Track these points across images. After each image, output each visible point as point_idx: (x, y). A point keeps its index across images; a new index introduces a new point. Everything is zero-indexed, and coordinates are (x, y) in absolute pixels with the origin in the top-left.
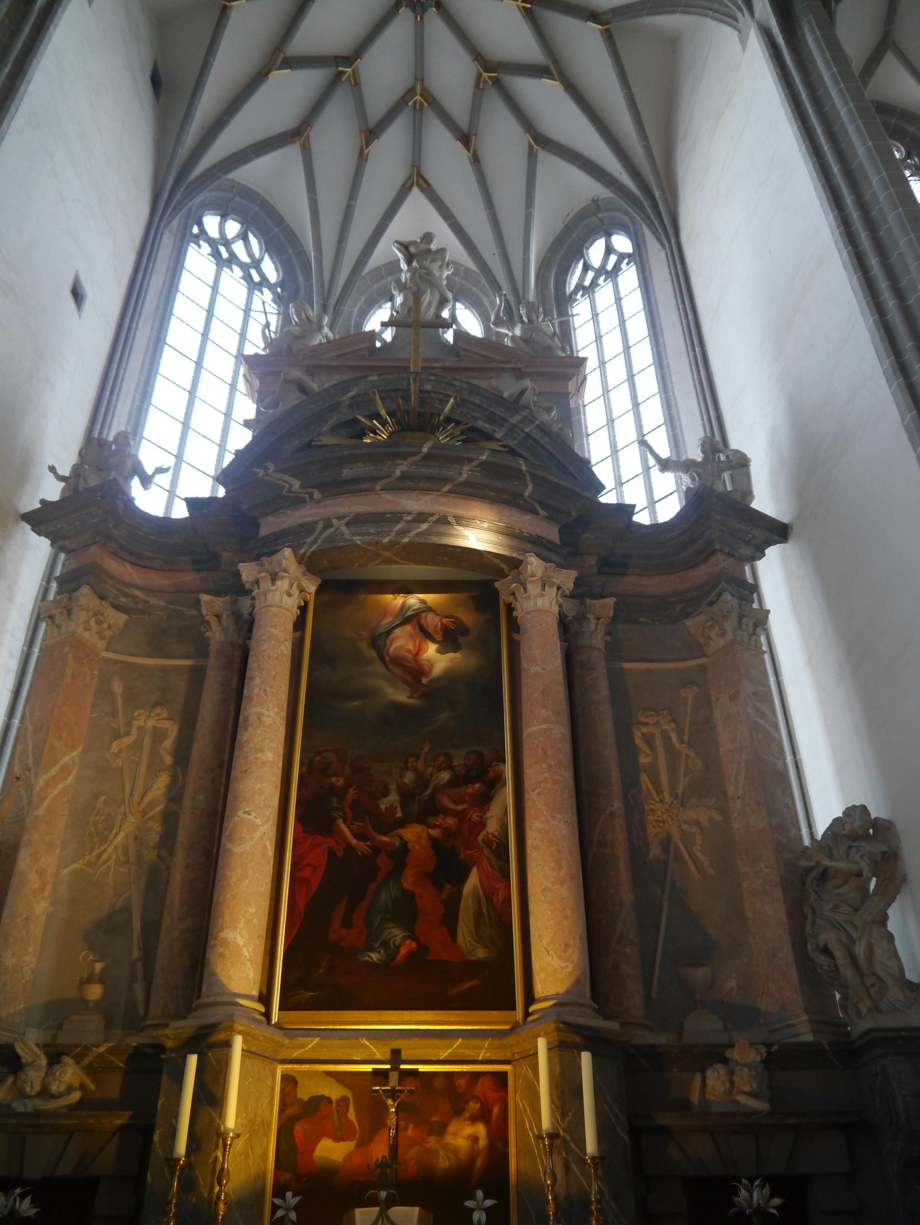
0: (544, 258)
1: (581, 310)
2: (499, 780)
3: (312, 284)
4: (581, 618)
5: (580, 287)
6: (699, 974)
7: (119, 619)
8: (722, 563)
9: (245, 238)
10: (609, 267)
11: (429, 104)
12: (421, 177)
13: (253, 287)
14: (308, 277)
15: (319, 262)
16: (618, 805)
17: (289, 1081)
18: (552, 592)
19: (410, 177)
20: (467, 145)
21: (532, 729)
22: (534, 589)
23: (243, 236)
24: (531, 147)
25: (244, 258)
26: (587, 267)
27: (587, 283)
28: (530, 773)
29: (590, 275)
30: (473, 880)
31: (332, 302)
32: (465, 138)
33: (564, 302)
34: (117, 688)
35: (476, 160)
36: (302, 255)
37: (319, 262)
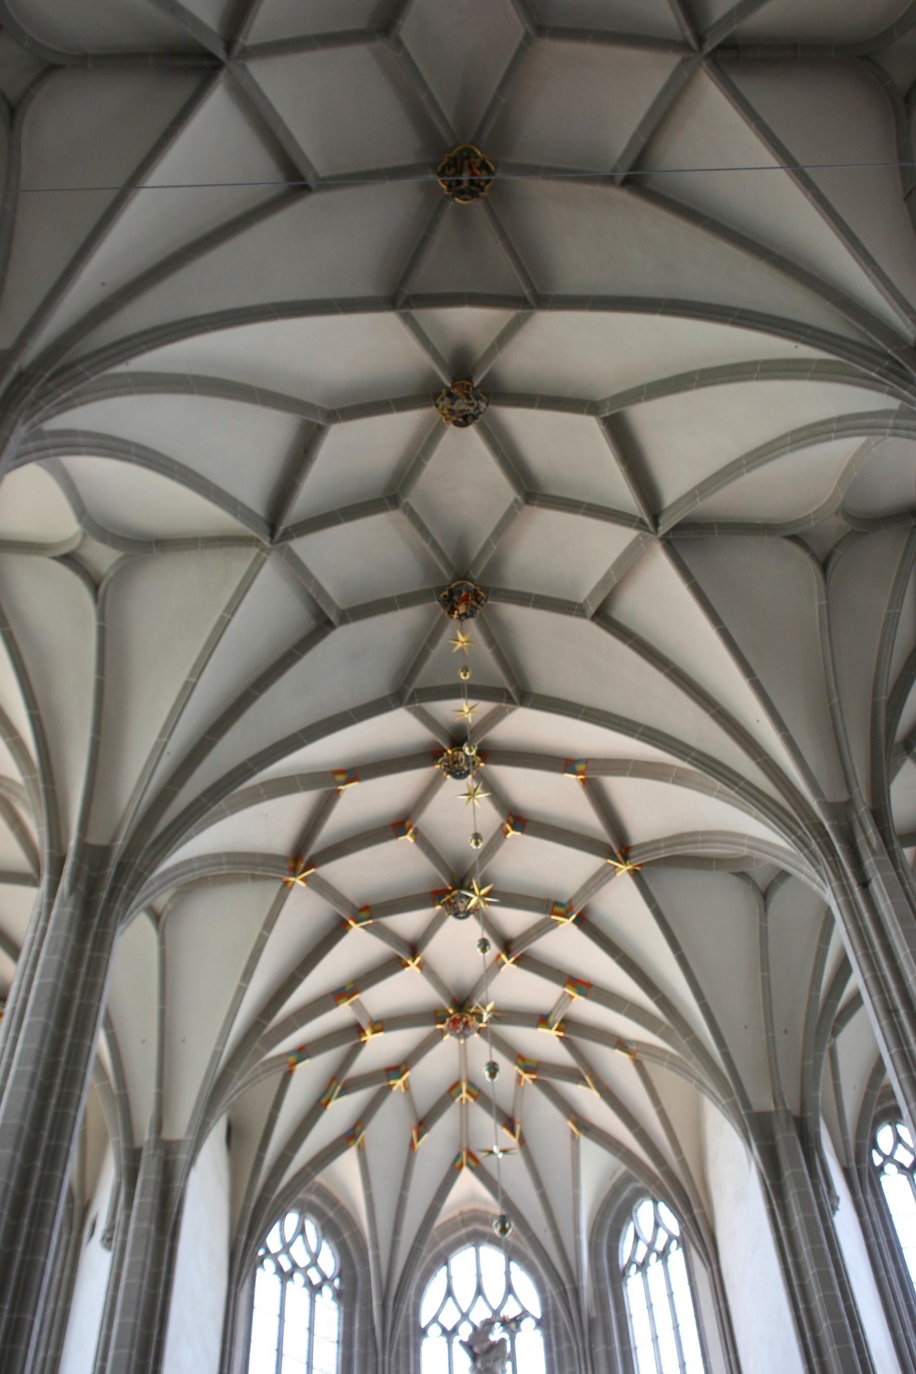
0: (595, 1221)
3: (369, 1271)
5: (631, 1261)
9: (302, 1231)
10: (659, 1246)
11: (475, 1098)
12: (470, 1155)
13: (315, 1290)
14: (365, 1262)
15: (376, 1246)
19: (459, 1156)
20: (512, 1130)
23: (302, 1231)
24: (573, 1134)
25: (303, 1260)
26: (637, 1238)
27: (639, 1258)
29: (642, 1250)
31: (391, 1303)
32: (509, 1123)
33: (618, 1276)
35: (522, 1141)
36: (357, 1235)
37: (377, 1257)
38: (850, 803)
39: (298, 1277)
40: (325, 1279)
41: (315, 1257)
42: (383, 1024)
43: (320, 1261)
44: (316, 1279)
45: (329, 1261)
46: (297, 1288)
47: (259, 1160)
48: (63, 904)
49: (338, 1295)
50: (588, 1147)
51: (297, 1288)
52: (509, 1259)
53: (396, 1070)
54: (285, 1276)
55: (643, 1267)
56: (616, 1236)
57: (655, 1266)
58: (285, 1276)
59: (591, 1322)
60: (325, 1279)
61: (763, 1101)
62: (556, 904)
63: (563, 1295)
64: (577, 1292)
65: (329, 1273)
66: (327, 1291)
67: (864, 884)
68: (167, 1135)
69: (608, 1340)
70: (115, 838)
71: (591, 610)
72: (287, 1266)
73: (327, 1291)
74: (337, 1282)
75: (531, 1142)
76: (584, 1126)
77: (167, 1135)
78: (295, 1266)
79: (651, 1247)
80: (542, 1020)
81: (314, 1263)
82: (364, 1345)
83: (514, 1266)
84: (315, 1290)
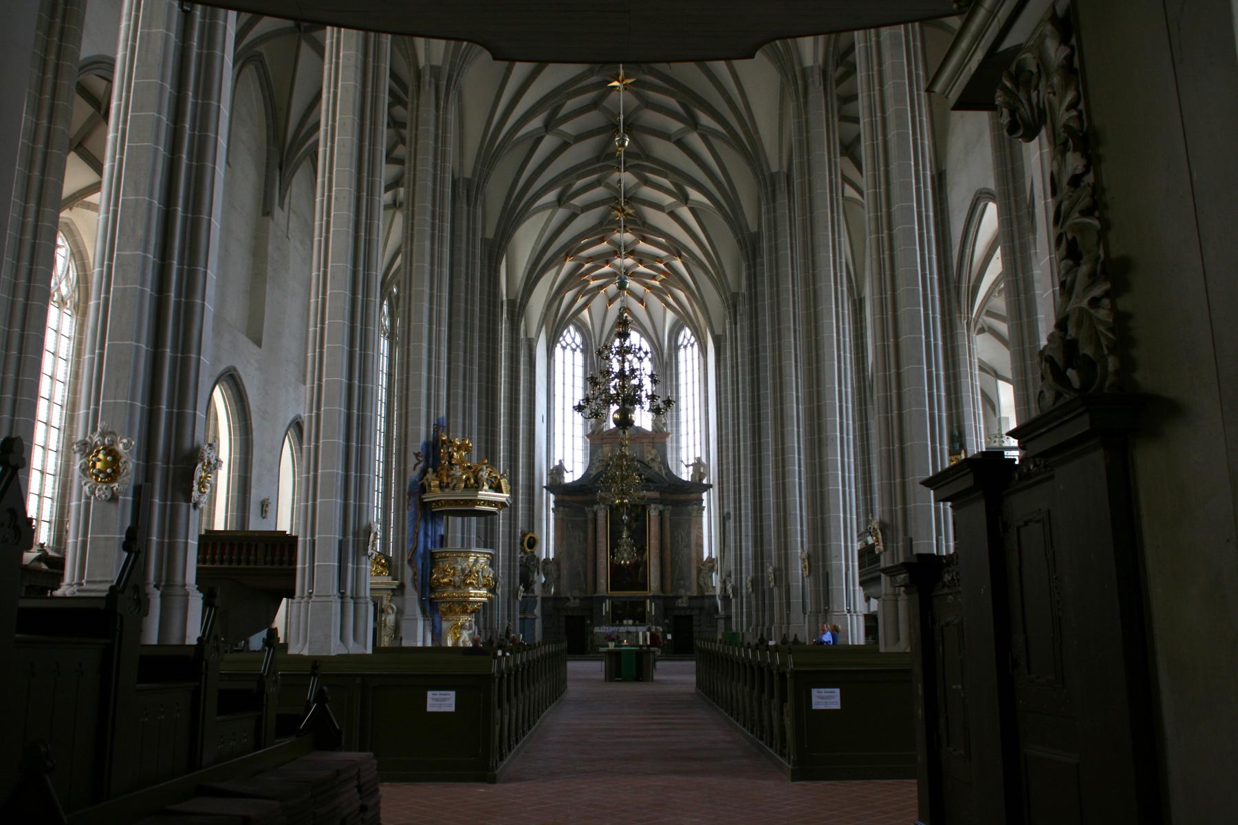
1: (682, 353)
2: (646, 550)
4: (664, 510)
6: (682, 582)
7: (567, 509)
8: (693, 496)
9: (569, 331)
13: (574, 350)
16: (669, 552)
17: (612, 603)
18: (657, 510)
21: (651, 542)
22: (652, 510)
26: (685, 337)
27: (685, 343)
28: (651, 551)
30: (641, 569)
32: (641, 301)
33: (677, 348)
34: (570, 526)
35: (646, 307)
36: (588, 330)
38: (738, 293)
39: (569, 347)
40: (578, 346)
41: (573, 339)
42: (595, 278)
43: (576, 340)
44: (574, 346)
45: (578, 340)
46: (568, 351)
47: (555, 320)
48: (506, 323)
49: (582, 351)
50: (668, 311)
51: (568, 351)
52: (641, 336)
53: (601, 287)
54: (564, 348)
55: (685, 347)
56: (678, 334)
57: (689, 347)
58: (564, 348)
59: (666, 363)
60: (578, 346)
61: (719, 331)
62: (658, 257)
63: (658, 354)
64: (662, 354)
65: (578, 344)
66: (578, 350)
67: (736, 324)
68: (529, 336)
69: (671, 370)
70: (517, 297)
71: (667, 211)
72: (564, 344)
73: (578, 350)
74: (581, 347)
75: (649, 306)
76: (668, 305)
77: (529, 336)
78: (567, 344)
79: (689, 340)
80: (654, 278)
81: (574, 342)
82: (590, 367)
83: (642, 339)
84: (574, 350)
